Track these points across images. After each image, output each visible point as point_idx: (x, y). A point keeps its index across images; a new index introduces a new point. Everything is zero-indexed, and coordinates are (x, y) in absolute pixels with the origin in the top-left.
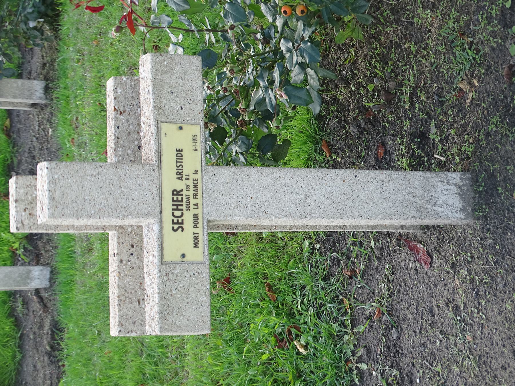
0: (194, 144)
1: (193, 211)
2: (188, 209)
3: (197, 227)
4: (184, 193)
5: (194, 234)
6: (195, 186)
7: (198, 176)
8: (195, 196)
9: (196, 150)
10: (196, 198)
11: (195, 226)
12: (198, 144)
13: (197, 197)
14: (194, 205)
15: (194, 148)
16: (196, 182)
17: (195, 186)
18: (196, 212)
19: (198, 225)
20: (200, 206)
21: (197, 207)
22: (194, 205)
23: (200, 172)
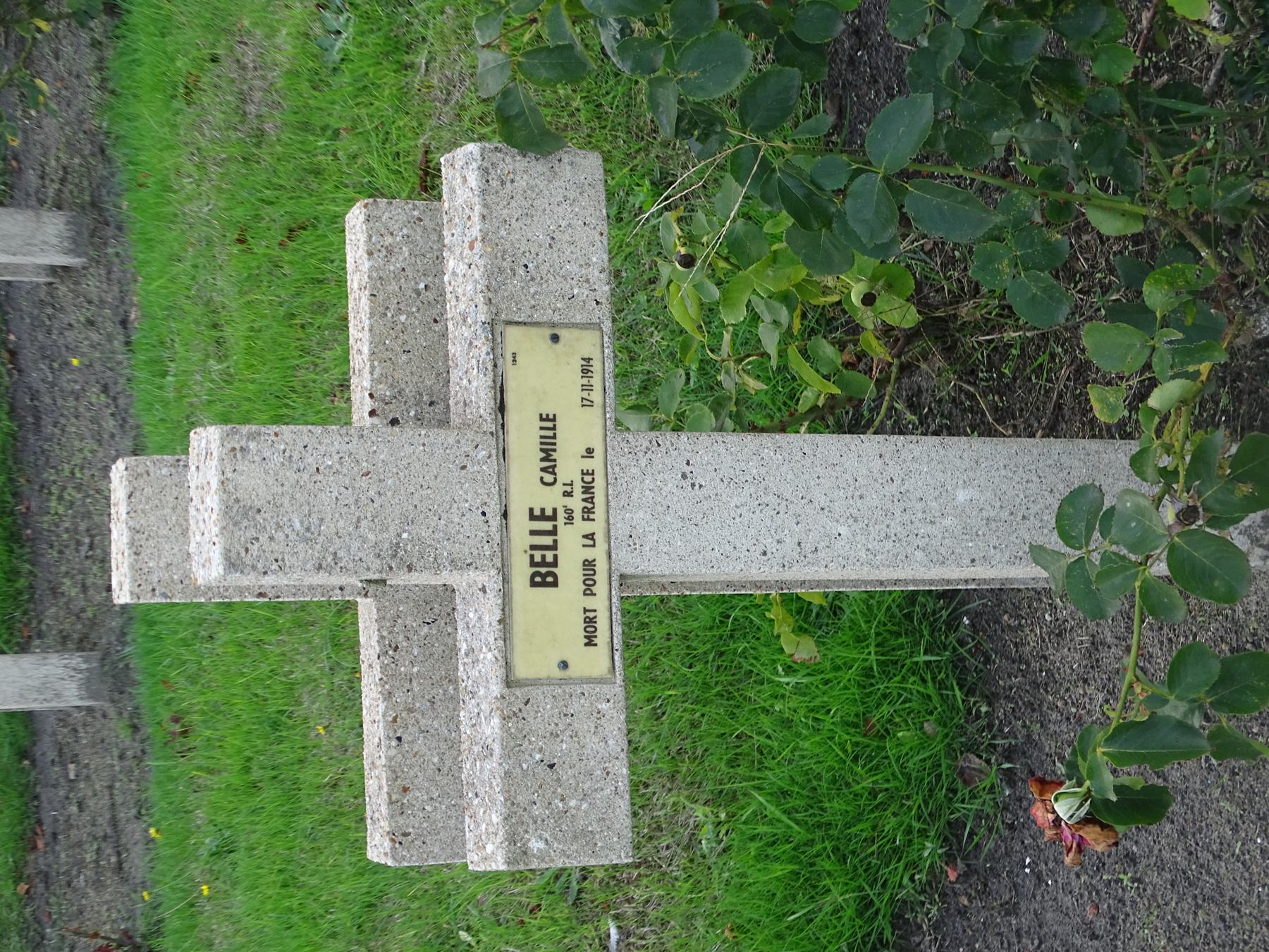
0: (585, 381)
5: (585, 610)
6: (588, 489)
7: (596, 464)
10: (589, 519)
11: (589, 592)
12: (596, 381)
13: (592, 516)
14: (585, 537)
17: (588, 489)
18: (589, 554)
20: (600, 538)
21: (591, 542)
22: (585, 537)
23: (599, 453)
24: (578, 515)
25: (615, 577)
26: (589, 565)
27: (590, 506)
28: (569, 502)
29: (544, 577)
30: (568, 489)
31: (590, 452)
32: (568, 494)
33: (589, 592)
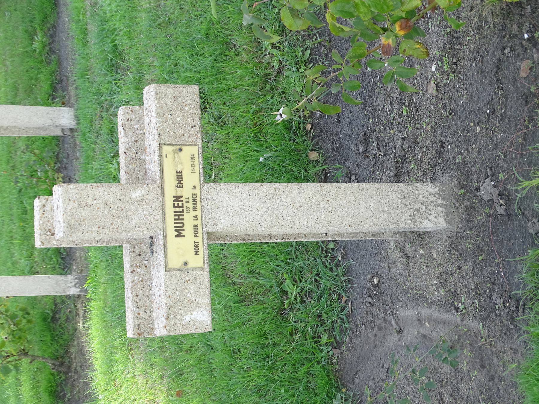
0: (192, 163)
3: (197, 237)
4: (185, 204)
5: (195, 242)
6: (194, 200)
8: (195, 209)
10: (195, 211)
11: (196, 236)
12: (196, 162)
14: (194, 217)
16: (194, 196)
17: (194, 200)
18: (196, 223)
20: (199, 217)
22: (194, 217)
23: (198, 187)
24: (191, 209)
29: (179, 235)
30: (187, 200)
32: (187, 202)
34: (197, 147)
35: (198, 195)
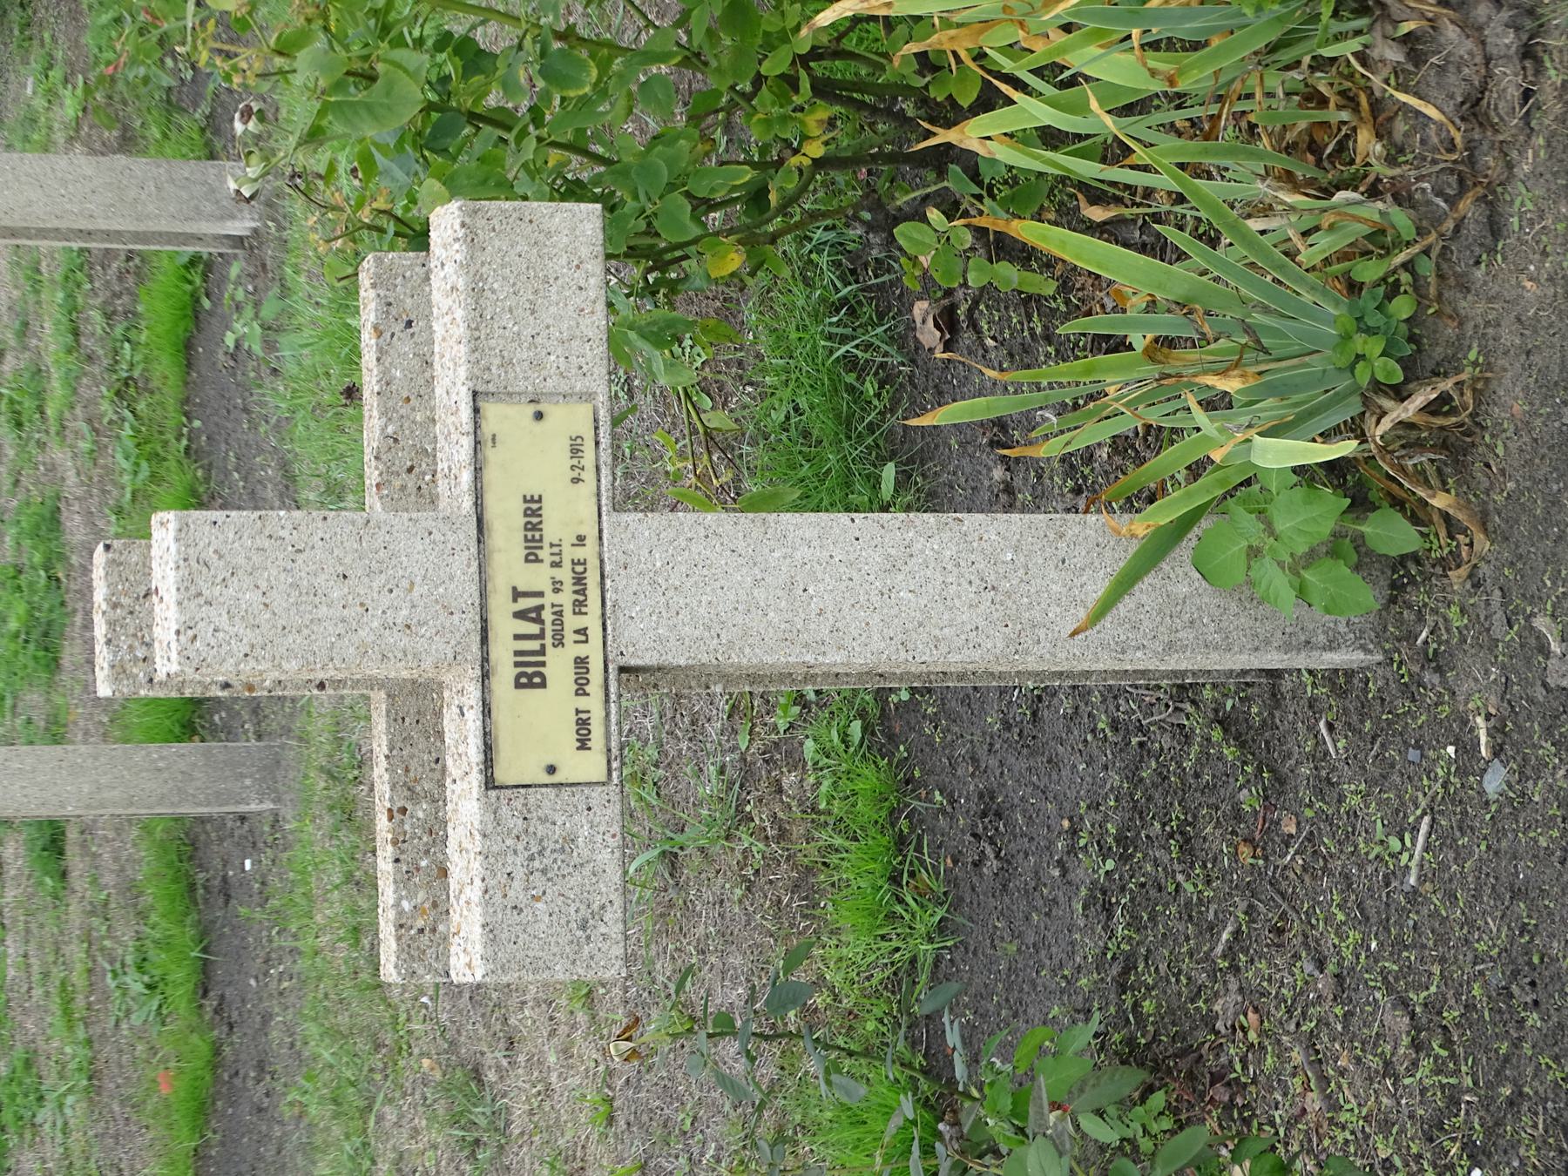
0: (575, 462)
1: (572, 650)
2: (559, 642)
5: (578, 712)
6: (579, 580)
9: (576, 480)
10: (581, 613)
11: (581, 691)
14: (577, 632)
15: (575, 474)
16: (579, 569)
17: (579, 580)
18: (582, 650)
19: (588, 689)
22: (577, 632)
23: (591, 541)
24: (568, 610)
25: (612, 676)
26: (581, 663)
27: (581, 598)
28: (557, 599)
31: (581, 539)
33: (581, 691)
34: (585, 411)
35: (588, 566)
